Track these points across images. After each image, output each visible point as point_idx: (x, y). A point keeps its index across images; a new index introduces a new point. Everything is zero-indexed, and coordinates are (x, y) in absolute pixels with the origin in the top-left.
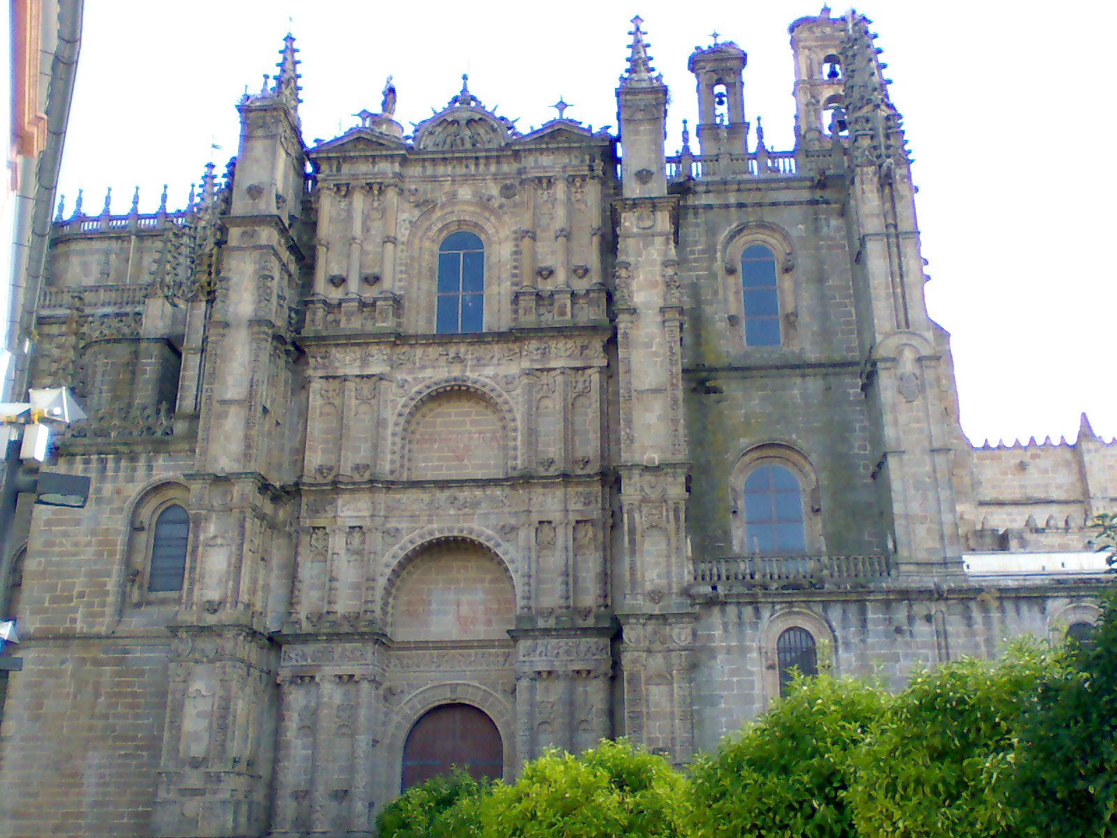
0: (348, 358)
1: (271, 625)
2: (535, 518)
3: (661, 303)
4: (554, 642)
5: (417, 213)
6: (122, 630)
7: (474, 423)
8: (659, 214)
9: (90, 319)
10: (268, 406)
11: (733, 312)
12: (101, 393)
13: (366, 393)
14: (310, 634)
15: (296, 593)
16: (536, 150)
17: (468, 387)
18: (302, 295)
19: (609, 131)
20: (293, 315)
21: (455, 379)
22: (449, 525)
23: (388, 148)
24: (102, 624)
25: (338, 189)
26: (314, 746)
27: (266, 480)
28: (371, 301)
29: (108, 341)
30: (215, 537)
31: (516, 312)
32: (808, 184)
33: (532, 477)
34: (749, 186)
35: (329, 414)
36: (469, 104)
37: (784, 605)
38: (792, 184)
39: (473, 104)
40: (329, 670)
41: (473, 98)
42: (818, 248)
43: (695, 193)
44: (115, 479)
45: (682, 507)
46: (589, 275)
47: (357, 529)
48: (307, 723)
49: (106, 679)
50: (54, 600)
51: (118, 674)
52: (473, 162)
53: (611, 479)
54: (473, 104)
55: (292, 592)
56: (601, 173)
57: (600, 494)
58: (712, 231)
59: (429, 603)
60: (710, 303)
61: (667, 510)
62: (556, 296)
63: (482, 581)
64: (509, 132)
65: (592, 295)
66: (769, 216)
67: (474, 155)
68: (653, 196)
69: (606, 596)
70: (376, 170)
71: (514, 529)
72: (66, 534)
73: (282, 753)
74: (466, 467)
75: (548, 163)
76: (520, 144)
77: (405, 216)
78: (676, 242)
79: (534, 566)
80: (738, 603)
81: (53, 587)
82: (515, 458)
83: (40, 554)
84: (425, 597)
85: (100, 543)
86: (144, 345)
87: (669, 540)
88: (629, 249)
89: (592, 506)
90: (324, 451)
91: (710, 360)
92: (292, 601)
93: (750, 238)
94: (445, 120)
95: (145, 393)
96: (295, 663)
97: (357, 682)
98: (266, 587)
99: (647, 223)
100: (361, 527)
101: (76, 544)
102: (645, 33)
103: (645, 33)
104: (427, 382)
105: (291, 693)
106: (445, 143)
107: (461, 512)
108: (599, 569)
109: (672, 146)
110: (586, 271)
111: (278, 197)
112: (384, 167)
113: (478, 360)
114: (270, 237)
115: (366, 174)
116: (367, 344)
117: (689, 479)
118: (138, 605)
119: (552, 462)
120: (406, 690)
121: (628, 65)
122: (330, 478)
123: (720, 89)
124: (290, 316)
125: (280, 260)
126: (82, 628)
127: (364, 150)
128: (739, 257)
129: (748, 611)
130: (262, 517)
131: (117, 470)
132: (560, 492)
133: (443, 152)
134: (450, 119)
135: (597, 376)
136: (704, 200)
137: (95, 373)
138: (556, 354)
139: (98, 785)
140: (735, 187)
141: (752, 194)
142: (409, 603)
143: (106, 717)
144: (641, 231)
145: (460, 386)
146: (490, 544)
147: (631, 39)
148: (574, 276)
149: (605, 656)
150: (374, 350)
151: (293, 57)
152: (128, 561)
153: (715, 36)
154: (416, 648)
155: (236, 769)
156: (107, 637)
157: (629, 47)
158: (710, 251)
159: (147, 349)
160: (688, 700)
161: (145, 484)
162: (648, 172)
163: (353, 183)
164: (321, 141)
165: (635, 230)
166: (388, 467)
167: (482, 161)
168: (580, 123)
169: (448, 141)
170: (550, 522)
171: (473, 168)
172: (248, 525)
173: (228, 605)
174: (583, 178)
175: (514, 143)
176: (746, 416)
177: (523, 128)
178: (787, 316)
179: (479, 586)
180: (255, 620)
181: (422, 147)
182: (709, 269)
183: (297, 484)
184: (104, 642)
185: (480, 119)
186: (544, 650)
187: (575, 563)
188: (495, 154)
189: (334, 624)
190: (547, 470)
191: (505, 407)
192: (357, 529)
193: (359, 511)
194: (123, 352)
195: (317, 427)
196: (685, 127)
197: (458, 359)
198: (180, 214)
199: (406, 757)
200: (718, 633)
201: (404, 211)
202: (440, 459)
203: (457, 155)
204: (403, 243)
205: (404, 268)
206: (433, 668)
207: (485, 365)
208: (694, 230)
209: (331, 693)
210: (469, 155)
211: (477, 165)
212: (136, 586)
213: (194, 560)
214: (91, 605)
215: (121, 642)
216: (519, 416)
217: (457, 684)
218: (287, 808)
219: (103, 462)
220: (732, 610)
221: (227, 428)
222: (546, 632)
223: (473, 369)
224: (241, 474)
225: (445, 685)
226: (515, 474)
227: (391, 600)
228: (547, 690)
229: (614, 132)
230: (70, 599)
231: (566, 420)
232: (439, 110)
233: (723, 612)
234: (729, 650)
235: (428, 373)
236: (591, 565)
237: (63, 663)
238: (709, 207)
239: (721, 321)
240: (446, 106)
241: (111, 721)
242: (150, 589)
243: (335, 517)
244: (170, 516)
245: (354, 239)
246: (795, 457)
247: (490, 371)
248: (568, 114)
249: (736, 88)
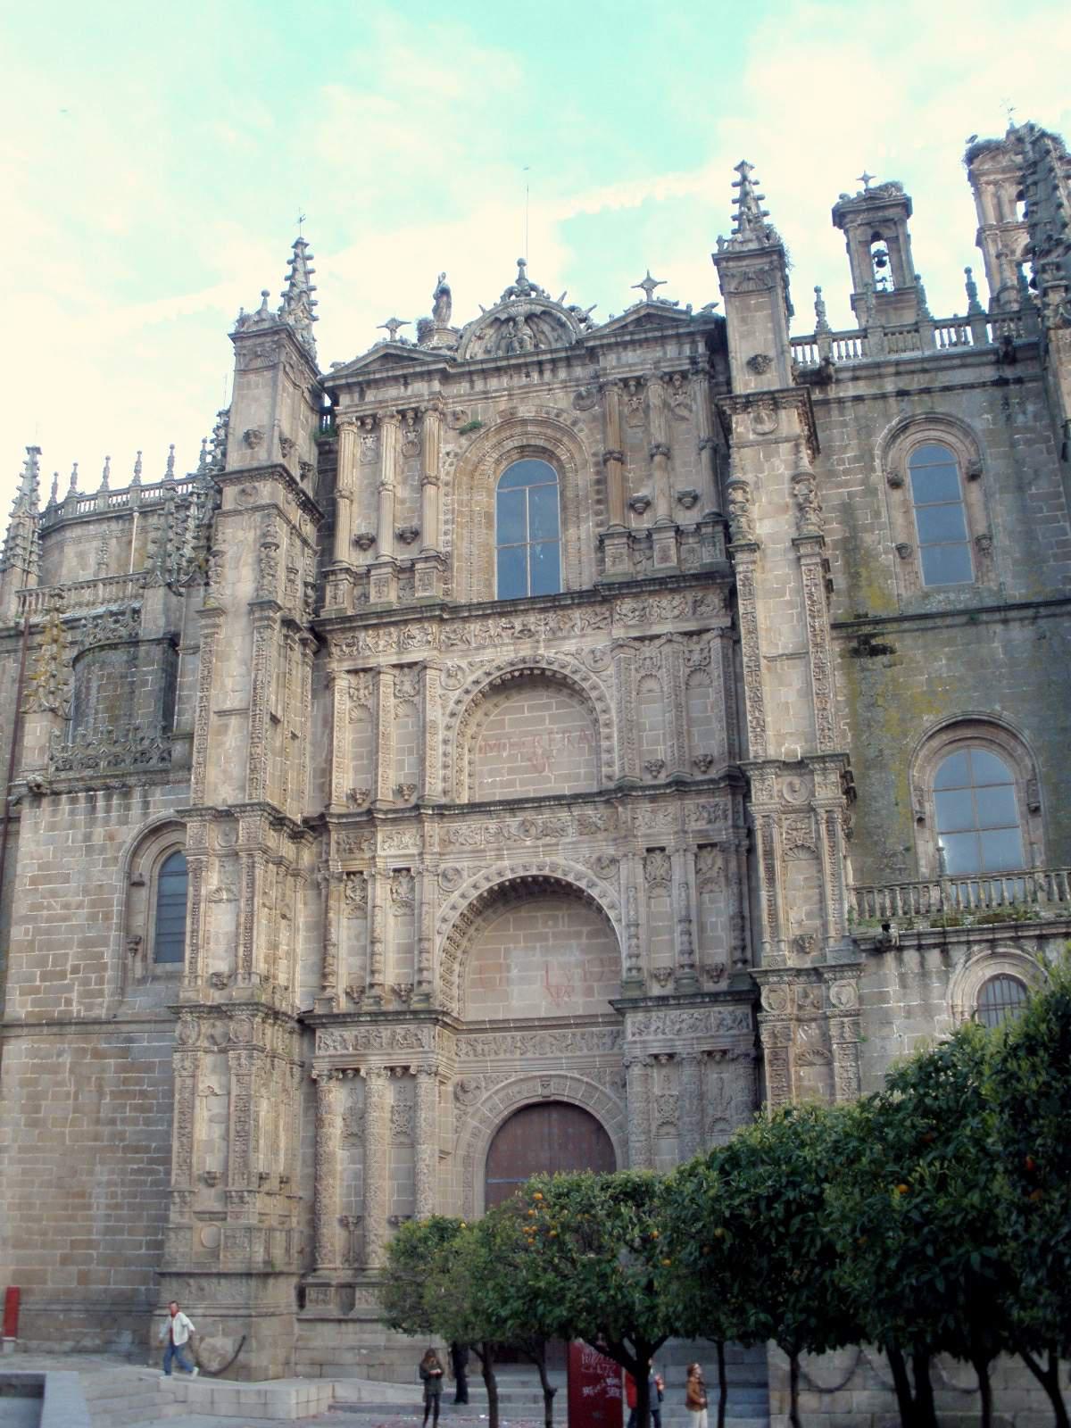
0: (382, 643)
1: (299, 1001)
2: (642, 844)
3: (794, 534)
4: (674, 1014)
5: (464, 441)
6: (125, 1012)
7: (553, 719)
8: (783, 413)
9: (83, 622)
10: (279, 715)
11: (901, 539)
12: (96, 713)
13: (407, 687)
14: (349, 1015)
15: (330, 960)
16: (617, 344)
17: (543, 670)
18: (321, 564)
19: (715, 311)
20: (310, 592)
21: (524, 661)
22: (526, 860)
23: (424, 363)
24: (101, 1005)
25: (363, 424)
26: (364, 1159)
27: (279, 812)
28: (408, 564)
29: (102, 648)
30: (219, 890)
31: (602, 561)
32: (992, 358)
33: (634, 788)
34: (912, 367)
35: (361, 720)
36: (529, 295)
37: (984, 945)
38: (969, 360)
39: (533, 294)
40: (376, 1061)
41: (533, 288)
42: (1013, 445)
43: (838, 381)
44: (107, 821)
45: (838, 816)
46: (699, 505)
47: (404, 873)
48: (355, 1129)
49: (110, 1075)
51: (123, 1068)
52: (536, 368)
53: (738, 783)
54: (533, 294)
55: (324, 960)
56: (707, 367)
57: (730, 806)
58: (865, 430)
59: (508, 969)
60: (870, 529)
61: (817, 823)
62: (655, 537)
63: (578, 935)
64: (582, 326)
65: (704, 530)
66: (942, 406)
67: (535, 359)
68: (773, 388)
69: (744, 948)
70: (409, 392)
71: (614, 861)
72: (54, 894)
73: (325, 1168)
74: (548, 780)
75: (634, 361)
76: (595, 338)
77: (449, 448)
78: (816, 450)
79: (642, 910)
80: (920, 948)
81: (42, 962)
82: (610, 764)
83: (26, 919)
84: (502, 961)
85: (93, 904)
86: (143, 648)
87: (820, 864)
88: (744, 463)
89: (718, 824)
90: (357, 770)
91: (875, 608)
92: (323, 972)
93: (919, 436)
94: (497, 319)
95: (145, 712)
96: (332, 1052)
97: (414, 1076)
98: (291, 954)
99: (767, 427)
100: (408, 870)
101: (66, 906)
102: (756, 183)
103: (756, 183)
104: (486, 668)
105: (330, 1091)
106: (498, 348)
107: (540, 843)
108: (732, 910)
109: (802, 324)
110: (696, 498)
111: (284, 441)
112: (420, 387)
113: (553, 631)
114: (272, 494)
115: (396, 399)
116: (406, 622)
117: (846, 776)
118: (143, 981)
119: (662, 765)
120: (483, 1084)
121: (735, 225)
122: (366, 806)
123: (880, 245)
124: (306, 595)
125: (288, 522)
126: (79, 1011)
127: (393, 369)
128: (906, 462)
129: (934, 957)
130: (279, 862)
131: (108, 810)
132: (673, 807)
133: (495, 360)
134: (503, 317)
135: (718, 641)
136: (850, 390)
137: (88, 688)
138: (659, 615)
139: (108, 1206)
140: (892, 370)
141: (916, 377)
142: (481, 970)
143: (113, 1122)
144: (761, 438)
145: (531, 669)
146: (582, 884)
147: (737, 193)
148: (680, 507)
149: (745, 1031)
150: (414, 629)
151: (305, 265)
152: (126, 927)
153: (865, 179)
154: (494, 1030)
155: (266, 1187)
156: (108, 1022)
157: (734, 202)
158: (866, 456)
159: (148, 653)
160: (854, 1085)
161: (141, 825)
162: (765, 357)
163: (380, 413)
164: (339, 364)
165: (752, 437)
166: (440, 786)
167: (548, 366)
168: (676, 304)
169: (503, 343)
170: (662, 849)
171: (535, 376)
172: (259, 872)
173: (240, 977)
174: (684, 375)
175: (588, 339)
176: (929, 681)
177: (599, 319)
178: (978, 540)
179: (574, 942)
180: (277, 996)
181: (468, 357)
182: (864, 482)
183: (322, 816)
184: (105, 1028)
185: (544, 313)
186: (660, 1025)
187: (700, 904)
188: (563, 354)
189: (378, 1000)
190: (655, 777)
191: (593, 694)
192: (404, 873)
193: (407, 847)
194: (118, 657)
195: (345, 738)
196: (818, 297)
197: (526, 632)
198: (191, 479)
199: (488, 1174)
200: (893, 988)
201: (447, 442)
202: (511, 771)
203: (513, 362)
204: (447, 484)
205: (449, 517)
206: (517, 1055)
207: (564, 638)
208: (840, 432)
209: (384, 1093)
210: (529, 359)
211: (541, 372)
212: (139, 957)
213: (195, 921)
214: (86, 982)
215: (125, 1028)
216: (613, 706)
217: (551, 1076)
218: (334, 1237)
219: (92, 800)
220: (911, 957)
221: (228, 744)
222: (662, 1001)
223: (547, 647)
224: (245, 805)
225: (535, 1077)
226: (612, 785)
227: (456, 967)
228: (668, 1079)
229: (720, 311)
230: (63, 975)
231: (678, 706)
232: (489, 307)
233: (900, 961)
234: (909, 1013)
235: (488, 654)
236: (722, 905)
237: (59, 1055)
238: (858, 399)
239: (886, 553)
240: (498, 301)
241: (119, 1128)
242: (156, 961)
243: (374, 858)
244: (169, 868)
245: (383, 484)
246: (1002, 737)
247: (570, 646)
248: (659, 293)
249: (899, 245)
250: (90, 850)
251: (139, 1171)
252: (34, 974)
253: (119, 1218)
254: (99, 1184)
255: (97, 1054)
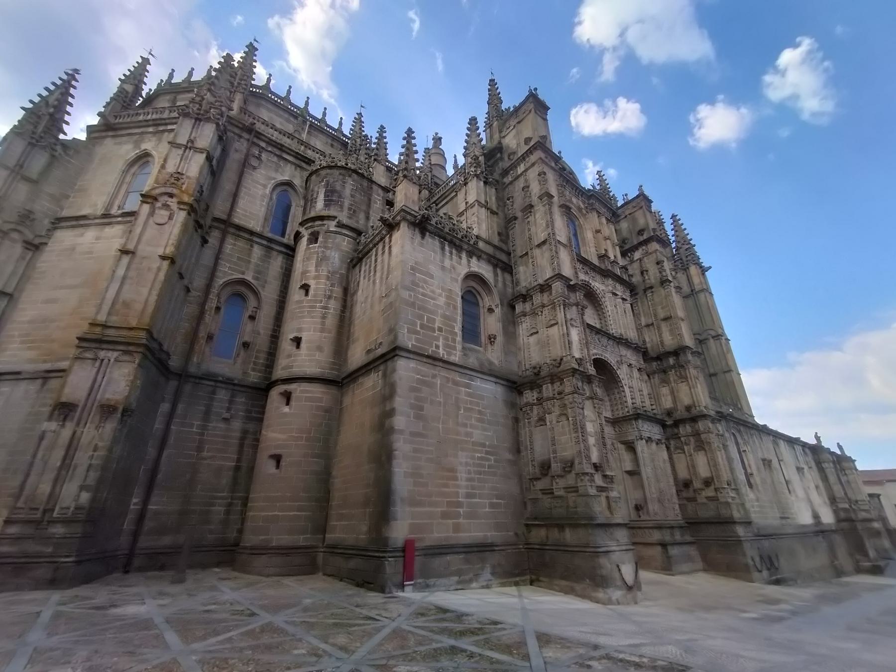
50: (422, 326)
101: (433, 292)
126: (443, 354)
131: (451, 253)
214: (446, 339)
230: (433, 330)
237: (434, 376)
250: (443, 268)
251: (479, 458)
252: (417, 323)
253: (473, 488)
254: (461, 464)
255: (456, 383)
